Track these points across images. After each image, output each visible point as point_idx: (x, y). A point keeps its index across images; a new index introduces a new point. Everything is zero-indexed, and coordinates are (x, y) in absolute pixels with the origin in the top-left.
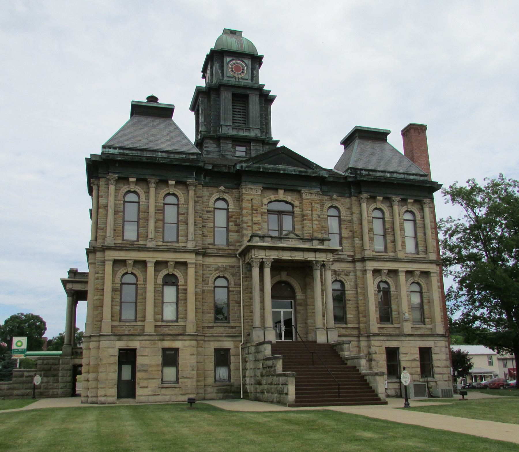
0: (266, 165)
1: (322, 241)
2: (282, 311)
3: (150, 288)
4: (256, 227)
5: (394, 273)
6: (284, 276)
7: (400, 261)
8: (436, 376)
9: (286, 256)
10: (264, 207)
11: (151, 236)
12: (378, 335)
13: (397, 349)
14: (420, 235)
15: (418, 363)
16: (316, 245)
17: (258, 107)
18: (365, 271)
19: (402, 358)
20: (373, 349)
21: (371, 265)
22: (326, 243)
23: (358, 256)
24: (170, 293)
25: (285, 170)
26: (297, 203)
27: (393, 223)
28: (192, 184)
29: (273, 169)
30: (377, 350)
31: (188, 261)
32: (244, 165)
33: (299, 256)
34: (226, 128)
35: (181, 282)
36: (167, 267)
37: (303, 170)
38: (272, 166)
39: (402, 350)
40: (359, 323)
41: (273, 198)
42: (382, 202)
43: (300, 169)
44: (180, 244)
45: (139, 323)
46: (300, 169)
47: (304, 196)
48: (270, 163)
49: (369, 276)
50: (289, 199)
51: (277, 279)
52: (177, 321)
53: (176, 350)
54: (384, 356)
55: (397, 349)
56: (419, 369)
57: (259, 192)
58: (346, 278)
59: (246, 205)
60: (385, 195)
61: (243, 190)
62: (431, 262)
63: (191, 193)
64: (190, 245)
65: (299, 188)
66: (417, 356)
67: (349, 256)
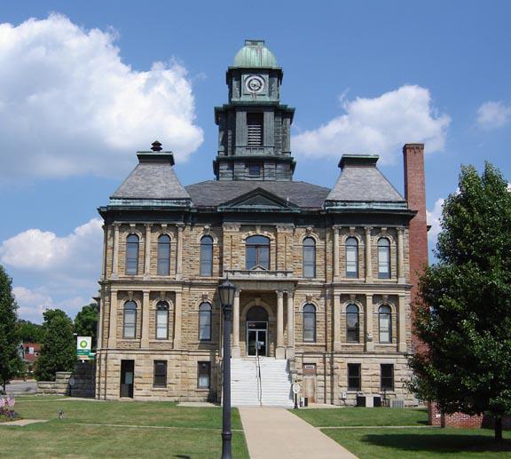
0: (244, 206)
1: (286, 273)
2: (257, 330)
3: (146, 312)
4: (234, 261)
5: (362, 298)
6: (258, 302)
7: (369, 287)
8: (396, 389)
9: (252, 287)
10: (243, 242)
11: (147, 271)
12: (341, 353)
13: (359, 365)
14: (394, 260)
15: (379, 378)
16: (280, 277)
17: (272, 124)
18: (332, 297)
19: (363, 372)
20: (335, 365)
21: (337, 292)
22: (289, 275)
23: (329, 283)
24: (162, 318)
25: (260, 209)
26: (272, 237)
27: (365, 250)
28: (180, 226)
29: (248, 209)
30: (339, 365)
31: (177, 291)
32: (223, 207)
33: (264, 288)
34: (241, 149)
35: (171, 308)
36: (159, 296)
37: (277, 207)
38: (249, 207)
39: (363, 366)
40: (326, 342)
41: (251, 233)
42: (355, 231)
43: (273, 207)
44: (171, 277)
45: (137, 340)
46: (273, 207)
47: (278, 231)
48: (246, 204)
49: (337, 300)
50: (266, 233)
51: (248, 307)
52: (167, 339)
53: (165, 362)
54: (346, 371)
55: (359, 365)
56: (379, 384)
57: (238, 230)
58: (317, 302)
59: (226, 241)
60: (358, 225)
61: (224, 229)
62: (400, 287)
63: (180, 234)
64: (178, 278)
65: (274, 224)
66: (379, 372)
67: (321, 282)
